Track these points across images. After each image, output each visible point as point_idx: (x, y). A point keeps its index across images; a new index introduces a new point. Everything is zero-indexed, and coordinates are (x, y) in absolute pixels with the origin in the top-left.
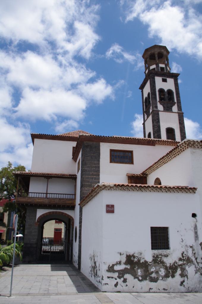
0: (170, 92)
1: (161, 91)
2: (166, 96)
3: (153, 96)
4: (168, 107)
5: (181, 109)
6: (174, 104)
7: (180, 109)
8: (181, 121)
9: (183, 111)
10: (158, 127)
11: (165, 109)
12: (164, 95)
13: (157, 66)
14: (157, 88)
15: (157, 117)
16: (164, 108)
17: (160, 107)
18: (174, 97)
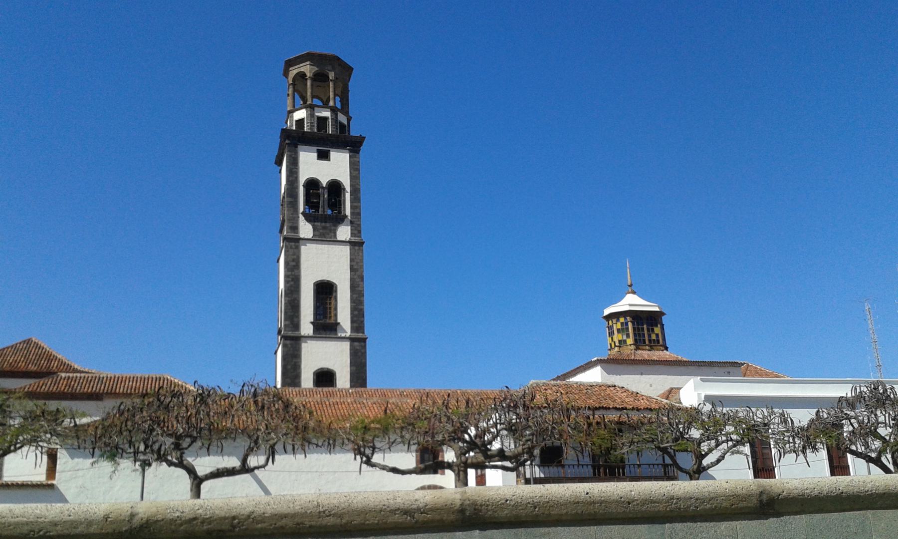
0: (335, 187)
1: (312, 184)
2: (322, 198)
3: (290, 199)
4: (324, 228)
5: (360, 232)
6: (339, 219)
7: (356, 232)
8: (354, 264)
9: (364, 237)
10: (293, 280)
11: (317, 233)
12: (318, 196)
13: (311, 115)
14: (303, 177)
15: (294, 254)
16: (314, 230)
17: (306, 229)
18: (344, 201)
